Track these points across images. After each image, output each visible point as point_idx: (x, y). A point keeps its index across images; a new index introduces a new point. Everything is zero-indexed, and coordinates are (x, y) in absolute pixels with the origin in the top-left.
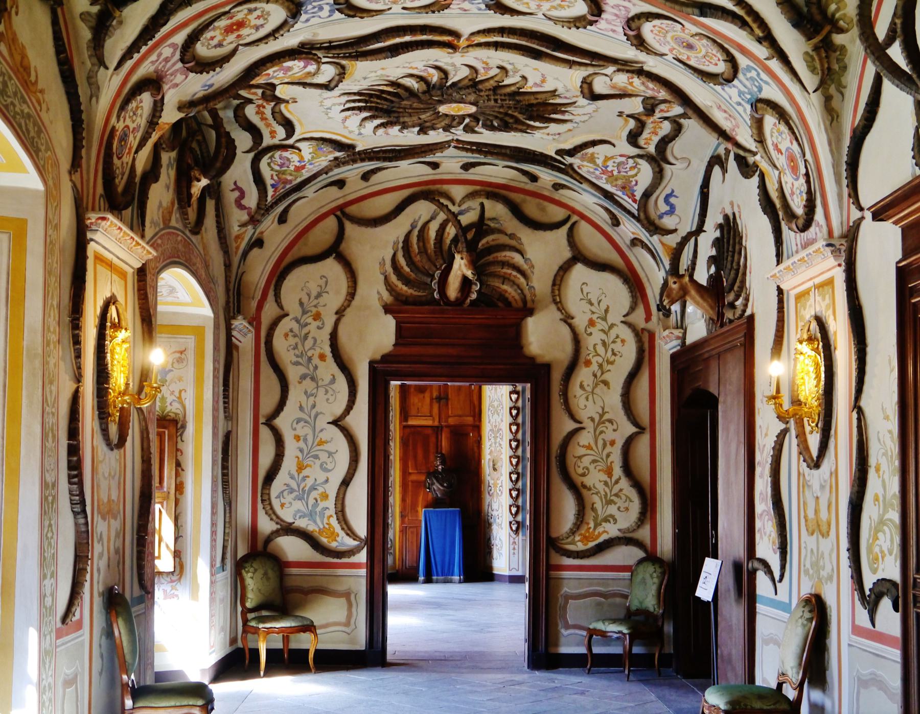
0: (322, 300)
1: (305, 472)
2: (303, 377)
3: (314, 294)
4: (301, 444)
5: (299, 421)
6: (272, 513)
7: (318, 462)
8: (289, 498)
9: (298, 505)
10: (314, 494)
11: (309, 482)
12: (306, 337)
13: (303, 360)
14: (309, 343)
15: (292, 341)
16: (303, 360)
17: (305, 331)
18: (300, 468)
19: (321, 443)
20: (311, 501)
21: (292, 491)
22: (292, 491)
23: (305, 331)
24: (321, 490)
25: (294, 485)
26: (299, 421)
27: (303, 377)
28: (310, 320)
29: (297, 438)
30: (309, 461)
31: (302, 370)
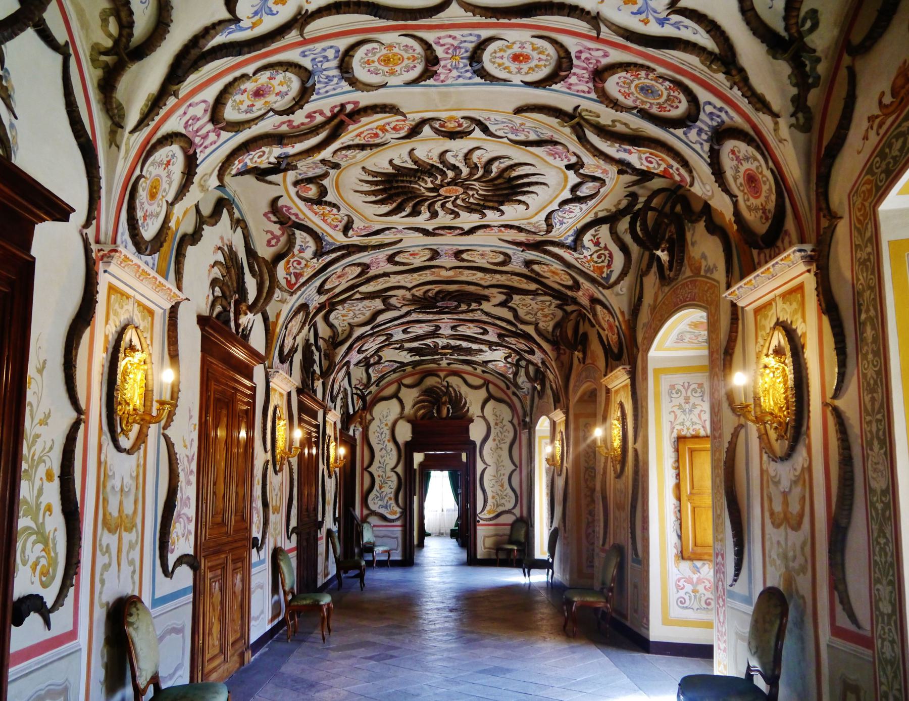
0: (388, 418)
1: (382, 490)
2: (381, 449)
3: (385, 415)
4: (381, 478)
5: (379, 467)
6: (368, 508)
7: (388, 485)
8: (376, 501)
9: (380, 503)
10: (387, 498)
11: (384, 494)
12: (382, 433)
13: (381, 443)
14: (383, 435)
15: (377, 435)
16: (381, 443)
17: (382, 430)
18: (381, 488)
19: (388, 477)
20: (385, 501)
21: (378, 497)
22: (378, 497)
23: (382, 430)
24: (389, 496)
25: (378, 495)
26: (379, 467)
27: (381, 449)
28: (384, 426)
29: (379, 476)
30: (384, 485)
31: (381, 446)
